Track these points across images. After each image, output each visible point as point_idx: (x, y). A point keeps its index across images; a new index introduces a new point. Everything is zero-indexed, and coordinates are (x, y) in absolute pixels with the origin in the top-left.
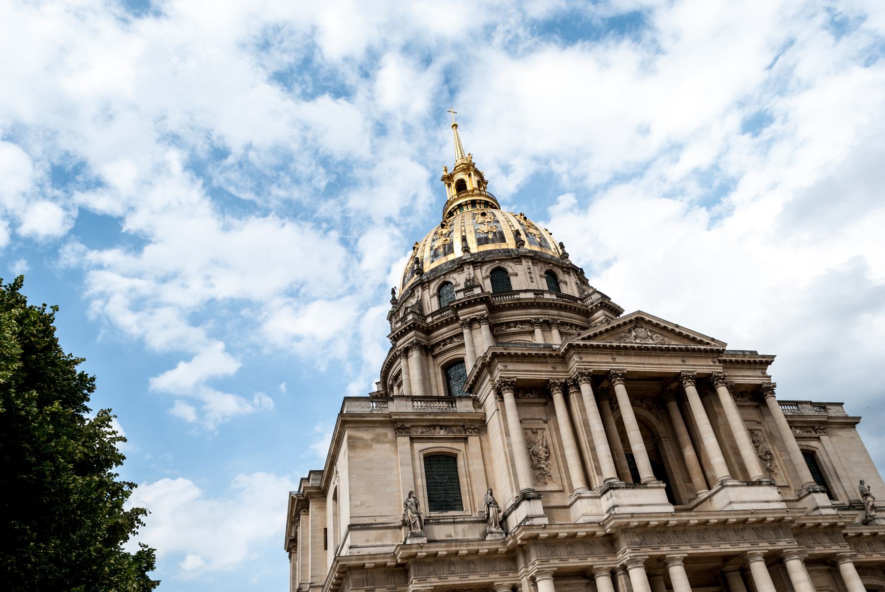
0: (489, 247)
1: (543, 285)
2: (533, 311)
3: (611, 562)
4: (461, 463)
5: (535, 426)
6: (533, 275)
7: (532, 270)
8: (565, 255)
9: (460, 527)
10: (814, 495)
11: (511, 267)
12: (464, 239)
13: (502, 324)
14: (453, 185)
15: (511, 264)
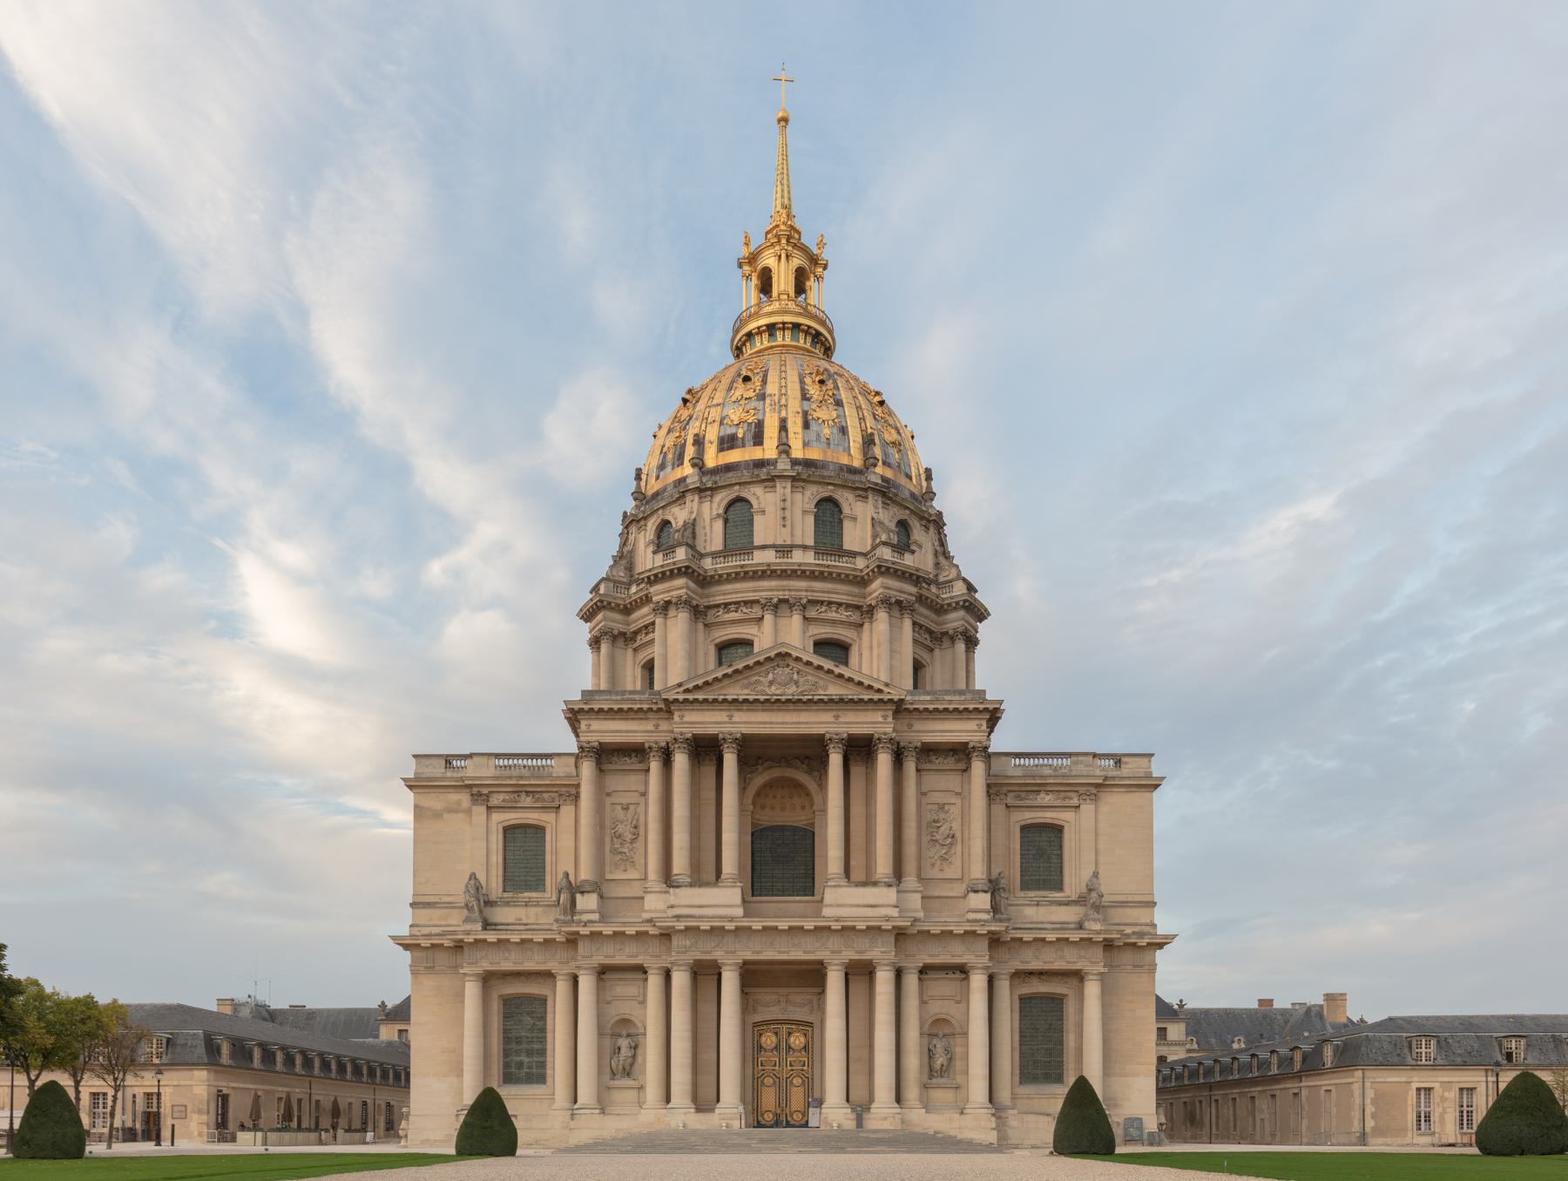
0: (734, 456)
1: (805, 530)
2: (765, 584)
3: (665, 962)
4: (548, 838)
5: (625, 801)
6: (788, 514)
7: (788, 504)
8: (870, 461)
9: (533, 911)
10: (972, 895)
11: (758, 496)
12: (699, 442)
13: (718, 606)
14: (755, 281)
15: (758, 490)
